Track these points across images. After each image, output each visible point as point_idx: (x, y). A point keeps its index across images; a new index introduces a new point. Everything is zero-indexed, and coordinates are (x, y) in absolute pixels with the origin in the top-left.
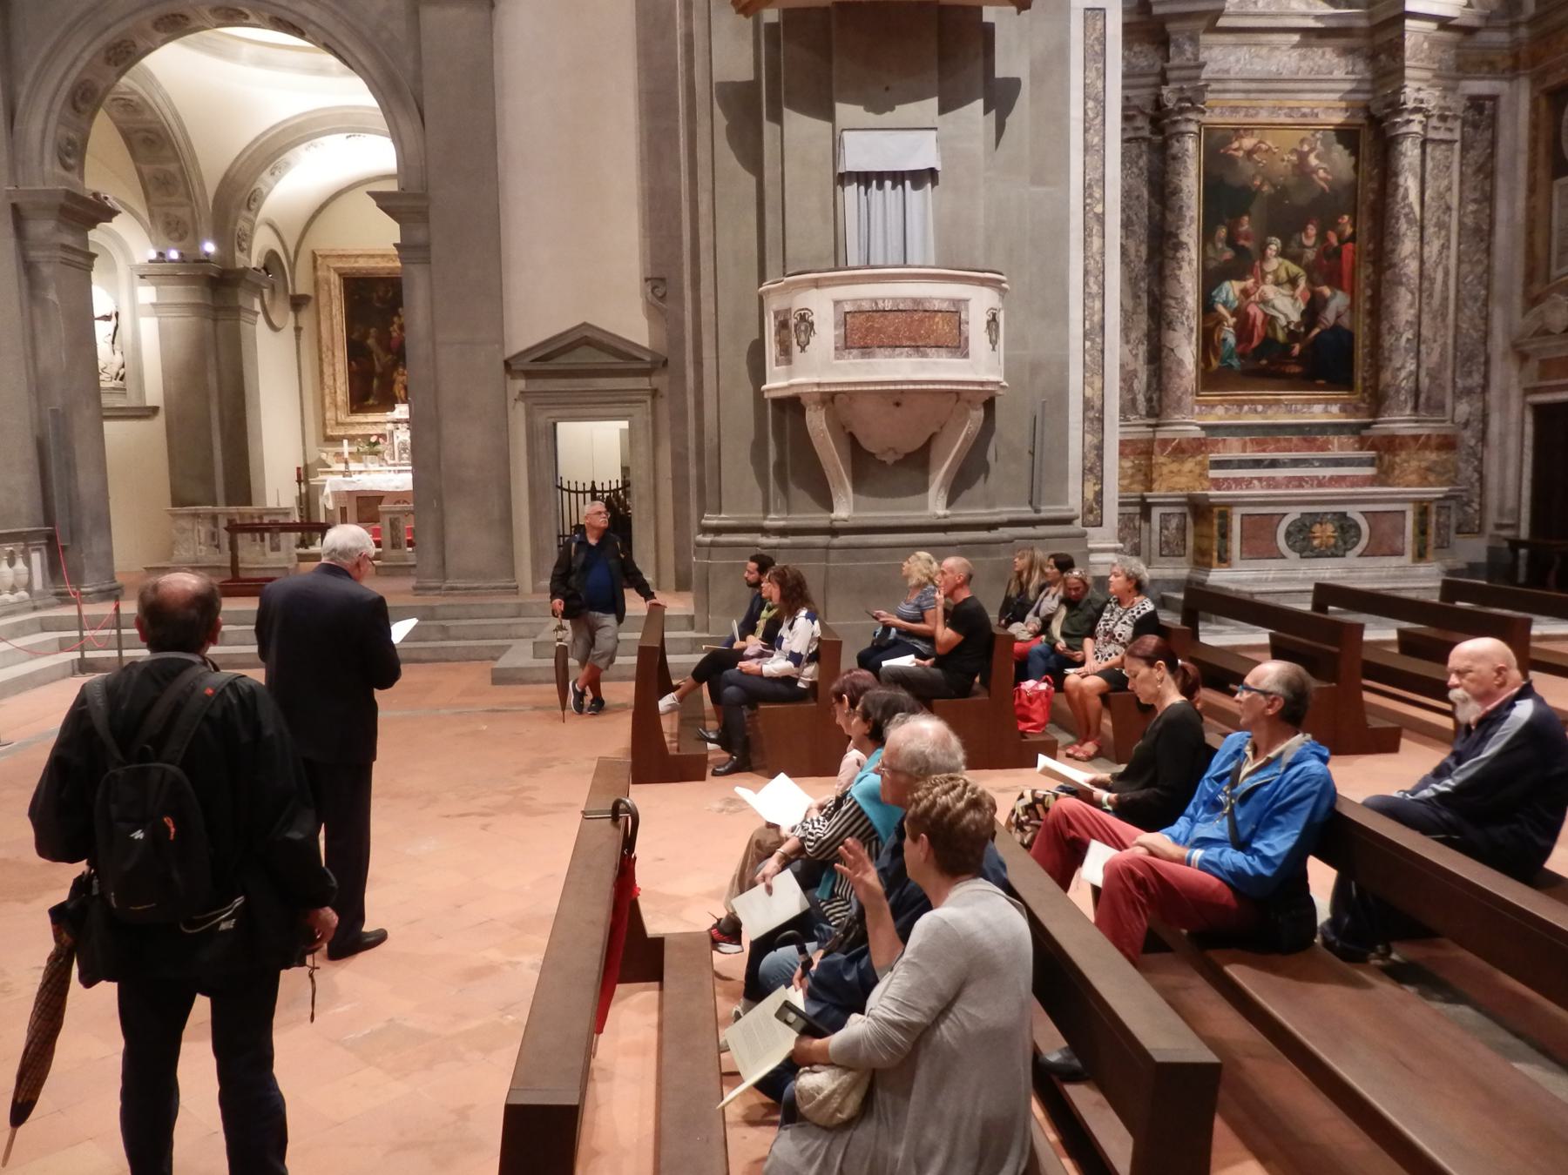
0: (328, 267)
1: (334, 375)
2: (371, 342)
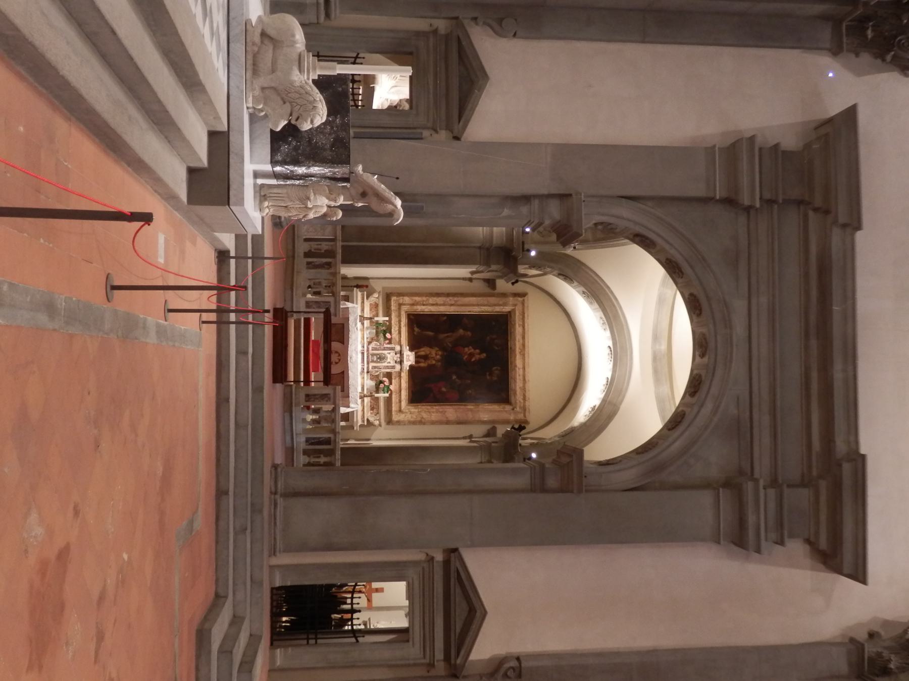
0: (515, 305)
1: (436, 304)
2: (461, 331)
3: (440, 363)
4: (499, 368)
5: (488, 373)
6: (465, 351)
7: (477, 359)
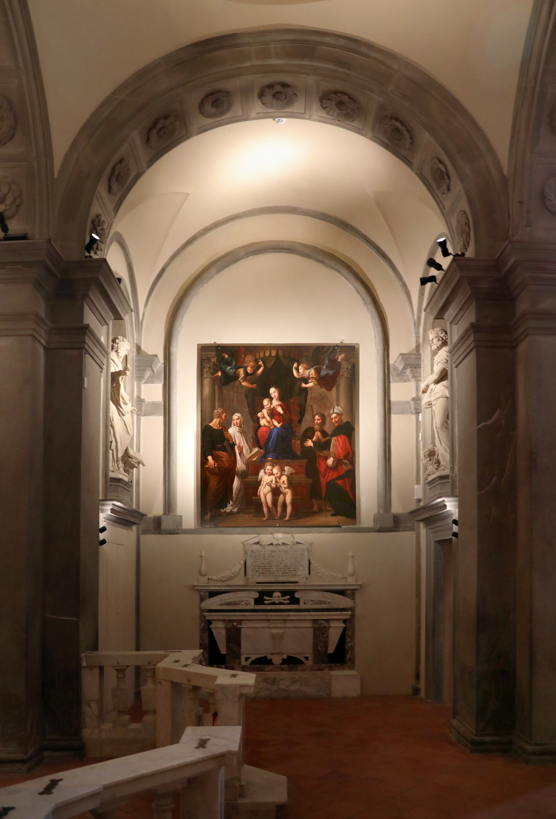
2: (233, 431)
3: (286, 468)
4: (295, 365)
5: (304, 385)
6: (267, 424)
7: (278, 403)
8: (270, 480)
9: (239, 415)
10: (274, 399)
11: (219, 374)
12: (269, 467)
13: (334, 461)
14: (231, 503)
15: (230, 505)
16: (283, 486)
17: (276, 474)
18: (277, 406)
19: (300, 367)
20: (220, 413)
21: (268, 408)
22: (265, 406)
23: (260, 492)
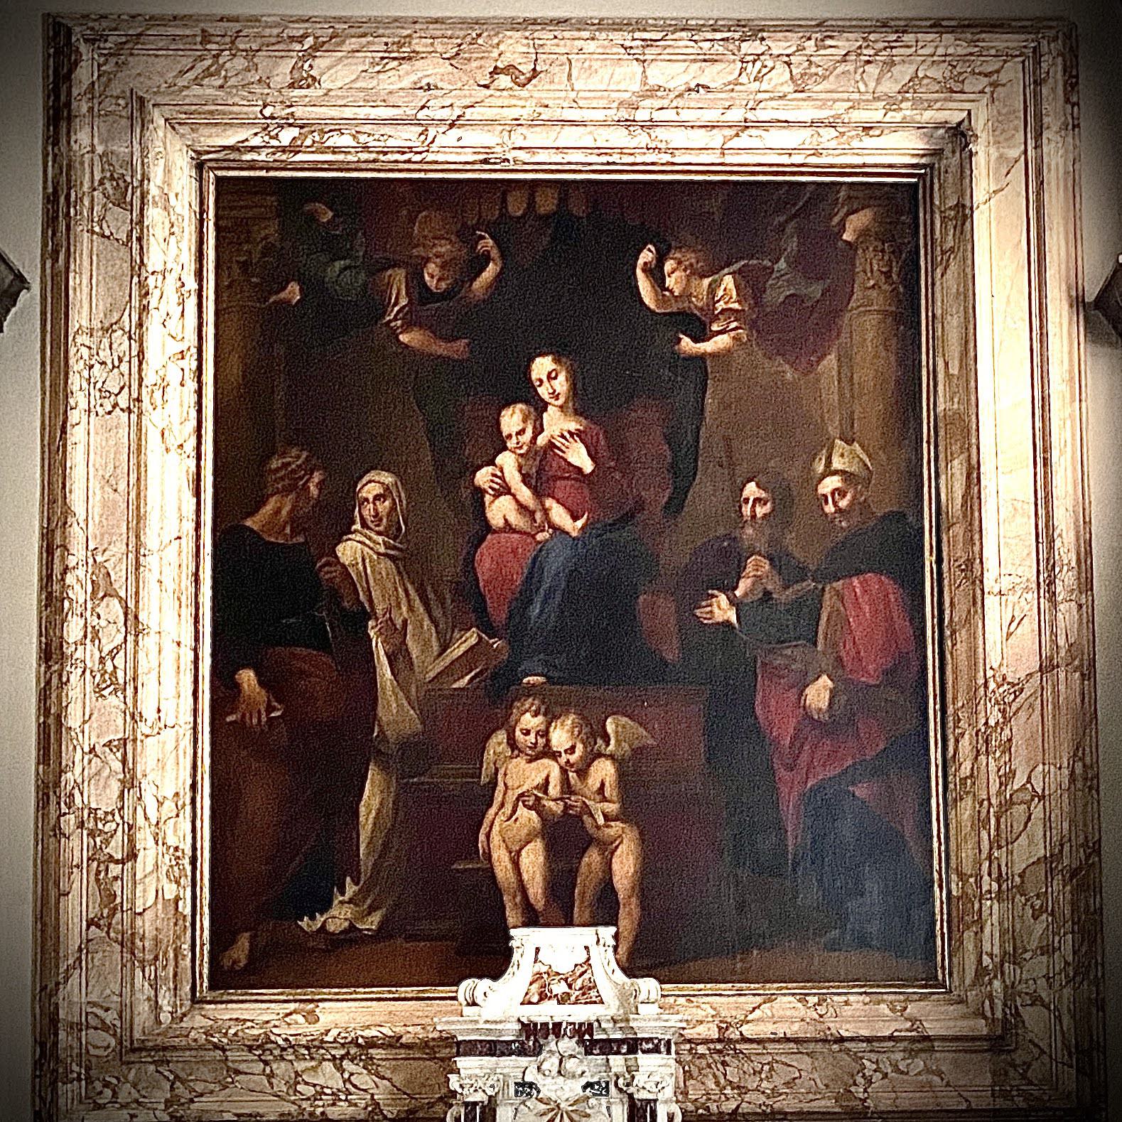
3: (610, 727)
4: (647, 256)
6: (515, 519)
7: (573, 426)
8: (539, 780)
9: (388, 478)
10: (550, 407)
11: (293, 292)
12: (530, 721)
13: (833, 694)
14: (350, 889)
15: (346, 898)
16: (598, 809)
17: (566, 751)
18: (563, 436)
19: (669, 265)
20: (293, 471)
21: (525, 448)
22: (510, 436)
23: (488, 836)
